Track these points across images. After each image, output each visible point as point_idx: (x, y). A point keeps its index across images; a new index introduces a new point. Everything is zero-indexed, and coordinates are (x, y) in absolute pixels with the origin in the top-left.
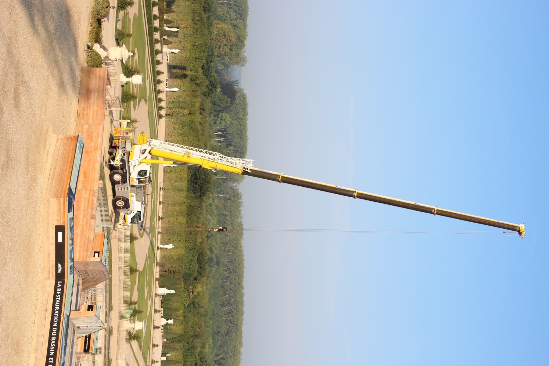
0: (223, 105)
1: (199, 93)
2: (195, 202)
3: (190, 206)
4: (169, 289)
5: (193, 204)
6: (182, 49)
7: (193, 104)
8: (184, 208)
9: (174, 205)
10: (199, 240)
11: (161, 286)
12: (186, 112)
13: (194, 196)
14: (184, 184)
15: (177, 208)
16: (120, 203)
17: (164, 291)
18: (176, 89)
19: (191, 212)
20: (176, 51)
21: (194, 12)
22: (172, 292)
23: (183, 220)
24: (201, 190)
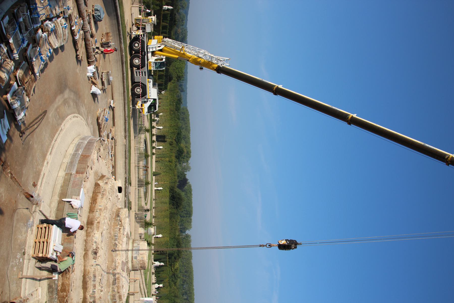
0: (183, 177)
1: (173, 151)
2: (174, 211)
3: (171, 213)
4: (160, 262)
5: (173, 212)
6: (164, 127)
7: (170, 157)
8: (168, 213)
9: (162, 212)
10: (177, 234)
11: (155, 261)
12: (167, 159)
13: (173, 207)
14: (167, 200)
15: (163, 213)
16: (139, 91)
17: (157, 263)
18: (161, 147)
19: (172, 216)
20: (161, 128)
21: (171, 110)
22: (162, 264)
23: (167, 220)
24: (177, 205)
